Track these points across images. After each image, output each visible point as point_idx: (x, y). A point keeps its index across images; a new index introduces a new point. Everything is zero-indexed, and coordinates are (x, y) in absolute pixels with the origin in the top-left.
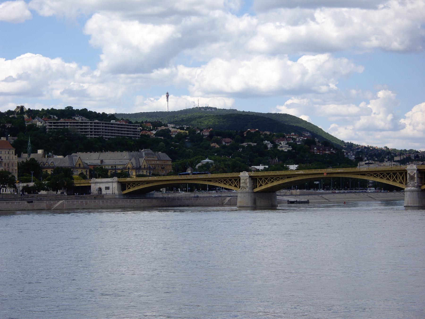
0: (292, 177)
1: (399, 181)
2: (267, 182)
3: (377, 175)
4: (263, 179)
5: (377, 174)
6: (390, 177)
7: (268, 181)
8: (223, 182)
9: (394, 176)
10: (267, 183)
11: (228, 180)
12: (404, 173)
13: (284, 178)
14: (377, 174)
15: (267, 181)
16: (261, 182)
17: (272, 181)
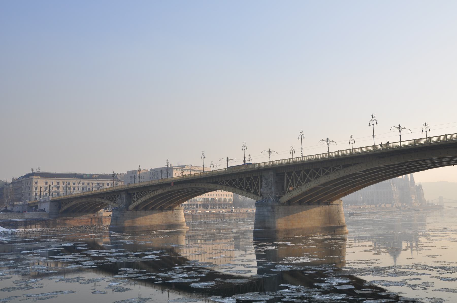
0: (350, 165)
1: (304, 182)
2: (319, 174)
3: (223, 183)
4: (311, 170)
5: (223, 181)
6: (229, 183)
7: (320, 173)
8: (225, 184)
9: (308, 175)
10: (309, 181)
11: (231, 180)
12: (259, 177)
13: (337, 168)
14: (223, 181)
15: (317, 173)
16: (308, 176)
17: (227, 184)
